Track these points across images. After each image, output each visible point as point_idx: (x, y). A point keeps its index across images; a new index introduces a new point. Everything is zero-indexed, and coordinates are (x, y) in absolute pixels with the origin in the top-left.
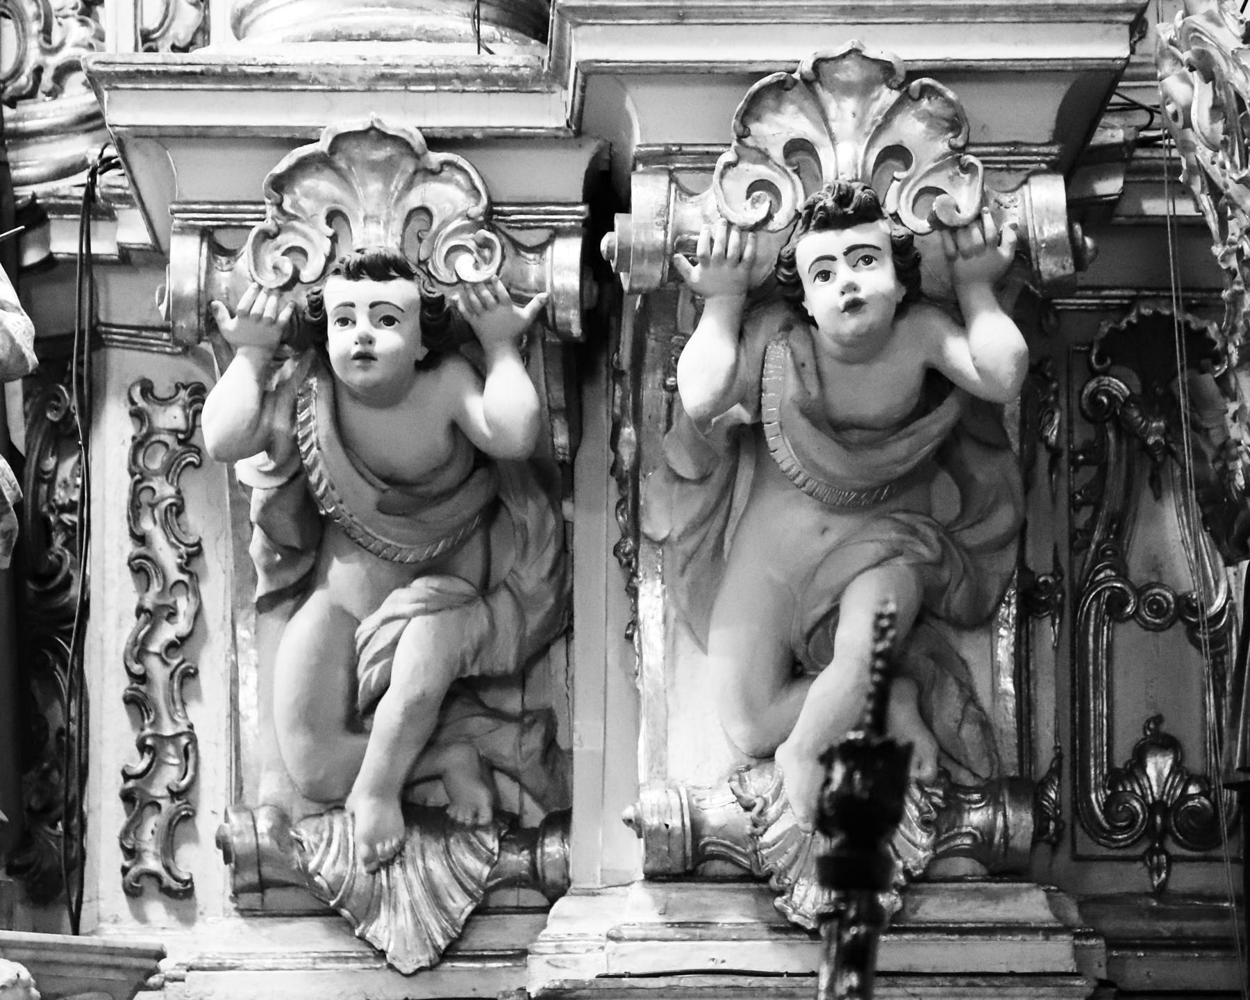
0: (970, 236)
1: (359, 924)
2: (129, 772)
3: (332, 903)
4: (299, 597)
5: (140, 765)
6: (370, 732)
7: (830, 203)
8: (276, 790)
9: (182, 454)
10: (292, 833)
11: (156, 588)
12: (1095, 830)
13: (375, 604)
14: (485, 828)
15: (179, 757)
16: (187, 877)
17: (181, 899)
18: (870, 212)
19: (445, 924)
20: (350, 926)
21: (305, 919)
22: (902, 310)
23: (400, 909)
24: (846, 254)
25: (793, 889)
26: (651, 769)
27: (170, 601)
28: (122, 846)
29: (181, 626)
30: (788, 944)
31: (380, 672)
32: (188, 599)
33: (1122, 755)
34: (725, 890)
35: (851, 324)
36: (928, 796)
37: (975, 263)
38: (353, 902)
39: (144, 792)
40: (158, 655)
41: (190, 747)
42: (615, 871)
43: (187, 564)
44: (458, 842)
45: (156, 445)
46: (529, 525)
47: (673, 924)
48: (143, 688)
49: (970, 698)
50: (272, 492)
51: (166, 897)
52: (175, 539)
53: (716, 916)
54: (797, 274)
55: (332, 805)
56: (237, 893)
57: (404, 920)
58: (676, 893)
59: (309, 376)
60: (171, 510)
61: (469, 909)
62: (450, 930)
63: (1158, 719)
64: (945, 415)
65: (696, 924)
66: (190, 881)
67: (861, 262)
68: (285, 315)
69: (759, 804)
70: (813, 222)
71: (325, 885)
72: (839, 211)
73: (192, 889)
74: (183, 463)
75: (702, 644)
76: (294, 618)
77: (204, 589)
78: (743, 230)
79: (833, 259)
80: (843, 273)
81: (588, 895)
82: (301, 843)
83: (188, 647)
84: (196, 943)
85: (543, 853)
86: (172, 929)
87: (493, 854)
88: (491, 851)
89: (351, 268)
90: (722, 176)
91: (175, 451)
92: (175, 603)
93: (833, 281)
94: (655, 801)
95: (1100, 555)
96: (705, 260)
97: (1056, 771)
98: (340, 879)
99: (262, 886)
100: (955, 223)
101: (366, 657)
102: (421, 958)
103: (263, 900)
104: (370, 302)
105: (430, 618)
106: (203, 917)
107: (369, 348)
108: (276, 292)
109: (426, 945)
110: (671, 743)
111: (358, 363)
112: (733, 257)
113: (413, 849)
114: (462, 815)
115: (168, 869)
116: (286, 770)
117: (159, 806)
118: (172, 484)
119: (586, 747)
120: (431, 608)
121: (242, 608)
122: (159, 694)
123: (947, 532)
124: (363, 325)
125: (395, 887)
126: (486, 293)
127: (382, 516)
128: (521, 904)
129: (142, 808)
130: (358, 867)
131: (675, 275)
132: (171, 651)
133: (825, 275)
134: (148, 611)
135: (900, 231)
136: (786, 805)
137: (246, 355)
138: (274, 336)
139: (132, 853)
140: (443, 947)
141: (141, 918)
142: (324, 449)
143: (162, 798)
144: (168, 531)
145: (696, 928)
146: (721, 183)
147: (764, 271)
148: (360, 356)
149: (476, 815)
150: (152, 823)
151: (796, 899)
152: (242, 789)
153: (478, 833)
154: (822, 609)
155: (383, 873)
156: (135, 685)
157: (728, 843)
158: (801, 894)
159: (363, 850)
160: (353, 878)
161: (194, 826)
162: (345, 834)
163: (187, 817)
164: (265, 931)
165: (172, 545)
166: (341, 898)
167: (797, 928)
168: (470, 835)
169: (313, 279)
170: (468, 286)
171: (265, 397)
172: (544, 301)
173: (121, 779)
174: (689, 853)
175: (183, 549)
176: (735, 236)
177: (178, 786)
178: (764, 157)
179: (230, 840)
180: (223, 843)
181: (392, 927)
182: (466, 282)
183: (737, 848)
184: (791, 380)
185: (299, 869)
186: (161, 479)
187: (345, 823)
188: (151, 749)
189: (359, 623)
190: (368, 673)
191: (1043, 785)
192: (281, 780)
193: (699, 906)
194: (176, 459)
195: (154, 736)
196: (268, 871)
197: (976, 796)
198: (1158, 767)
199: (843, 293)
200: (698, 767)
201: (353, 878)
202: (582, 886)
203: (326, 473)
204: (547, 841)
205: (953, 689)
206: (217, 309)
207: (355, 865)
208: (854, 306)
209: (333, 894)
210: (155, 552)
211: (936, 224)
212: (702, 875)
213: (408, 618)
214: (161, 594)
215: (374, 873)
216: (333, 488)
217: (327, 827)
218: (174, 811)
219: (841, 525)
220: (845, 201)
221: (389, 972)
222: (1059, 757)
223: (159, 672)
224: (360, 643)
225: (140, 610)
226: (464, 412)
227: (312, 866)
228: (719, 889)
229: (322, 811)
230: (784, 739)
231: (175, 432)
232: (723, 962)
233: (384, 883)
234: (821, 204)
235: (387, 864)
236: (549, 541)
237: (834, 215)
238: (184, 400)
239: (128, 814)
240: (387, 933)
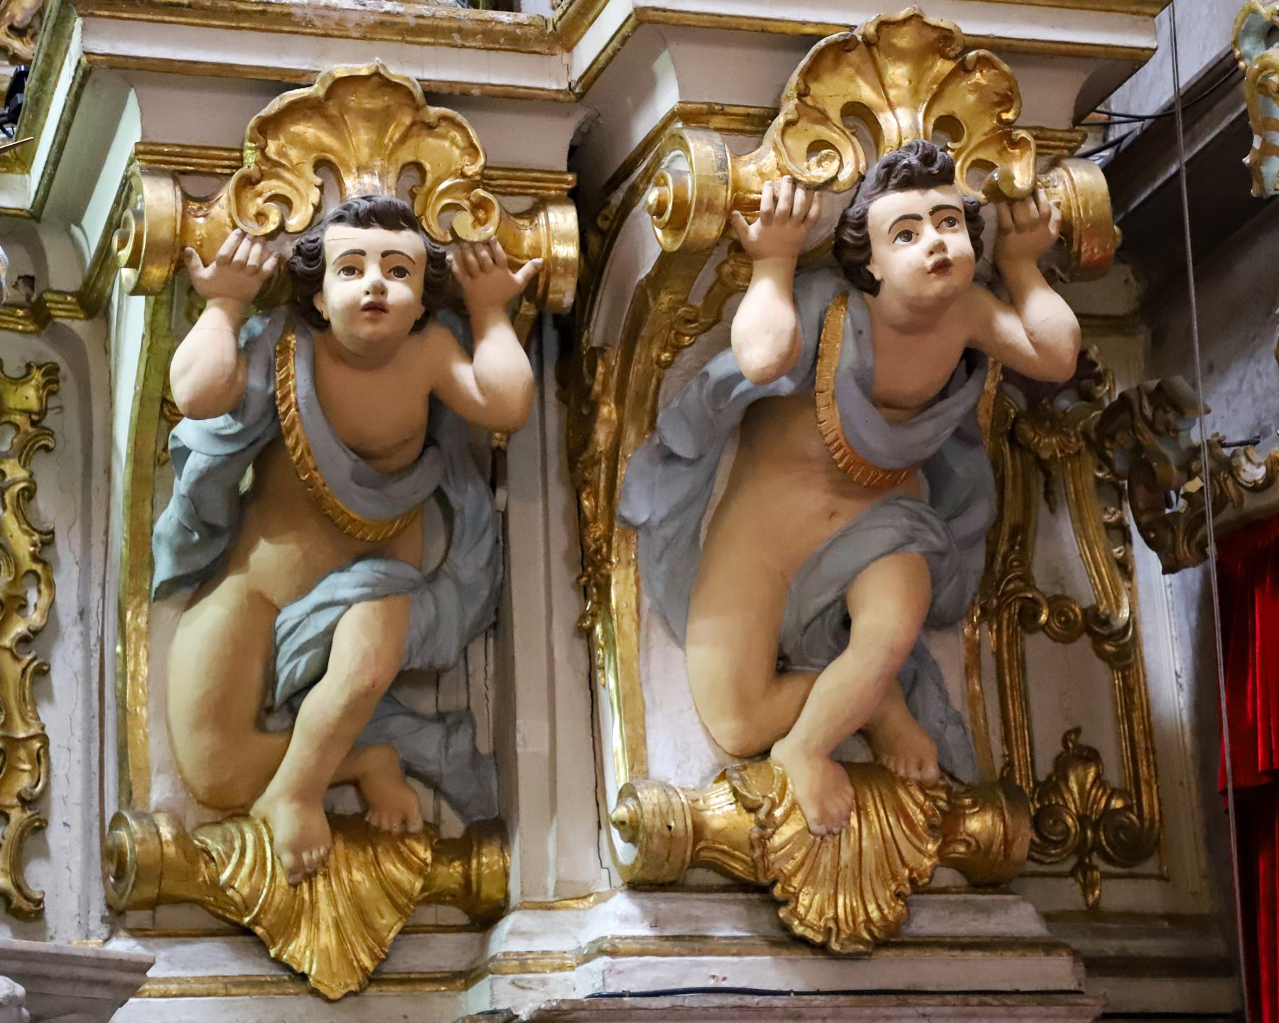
0: (1028, 209)
1: (274, 945)
3: (247, 919)
4: (197, 585)
9: (36, 436)
13: (304, 590)
14: (416, 836)
15: (31, 762)
16: (39, 896)
19: (371, 942)
20: (262, 945)
23: (323, 926)
24: (931, 214)
25: (797, 899)
26: (632, 769)
29: (35, 618)
30: (789, 960)
31: (307, 664)
32: (39, 592)
34: (713, 901)
36: (934, 799)
37: (1028, 238)
40: (10, 650)
42: (571, 882)
44: (388, 851)
45: (7, 426)
46: (467, 511)
47: (667, 938)
50: (219, 460)
52: (29, 526)
53: (709, 929)
54: (867, 236)
55: (230, 813)
57: (327, 938)
58: (665, 904)
59: (286, 332)
60: (23, 494)
61: (397, 927)
62: (377, 950)
65: (692, 938)
66: (41, 901)
67: (944, 224)
68: (269, 265)
70: (893, 181)
74: (37, 446)
75: (678, 638)
76: (196, 608)
77: (58, 580)
78: (811, 188)
79: (918, 218)
80: (929, 235)
81: (541, 908)
82: (209, 853)
83: (38, 642)
85: (480, 864)
87: (426, 864)
88: (424, 861)
89: (361, 215)
91: (26, 432)
93: (916, 242)
94: (655, 801)
96: (768, 218)
100: (1014, 196)
101: (287, 649)
102: (349, 981)
103: (154, 917)
104: (383, 250)
105: (376, 604)
107: (381, 298)
108: (261, 240)
110: (648, 741)
111: (367, 314)
112: (800, 214)
113: (337, 860)
114: (387, 821)
115: (18, 888)
116: (180, 771)
118: (24, 467)
119: (530, 749)
120: (376, 593)
124: (373, 273)
125: (317, 902)
126: (484, 253)
127: (355, 487)
128: (440, 923)
130: (278, 879)
133: (908, 236)
136: (794, 805)
137: (221, 306)
138: (254, 286)
140: (371, 969)
142: (303, 411)
144: (21, 518)
145: (695, 943)
146: (783, 140)
148: (369, 307)
149: (405, 822)
151: (801, 910)
153: (407, 841)
155: (305, 886)
157: (725, 847)
158: (806, 903)
161: (45, 841)
165: (25, 532)
166: (258, 914)
167: (803, 942)
168: (399, 844)
169: (300, 228)
170: (466, 245)
171: (245, 352)
172: (540, 267)
174: (688, 860)
175: (36, 537)
176: (800, 194)
177: (31, 794)
182: (464, 241)
183: (737, 853)
184: (850, 346)
186: (14, 461)
189: (279, 612)
190: (291, 666)
192: (173, 783)
193: (689, 918)
194: (29, 441)
199: (931, 253)
200: (678, 767)
202: (532, 899)
203: (302, 437)
204: (484, 851)
206: (190, 256)
209: (248, 908)
210: (6, 539)
212: (683, 885)
215: (295, 886)
216: (309, 453)
220: (929, 160)
224: (282, 632)
226: (451, 381)
227: (224, 877)
228: (707, 900)
229: (220, 819)
231: (28, 412)
232: (724, 979)
233: (307, 897)
234: (905, 162)
235: (310, 877)
236: (485, 530)
237: (920, 173)
238: (37, 380)
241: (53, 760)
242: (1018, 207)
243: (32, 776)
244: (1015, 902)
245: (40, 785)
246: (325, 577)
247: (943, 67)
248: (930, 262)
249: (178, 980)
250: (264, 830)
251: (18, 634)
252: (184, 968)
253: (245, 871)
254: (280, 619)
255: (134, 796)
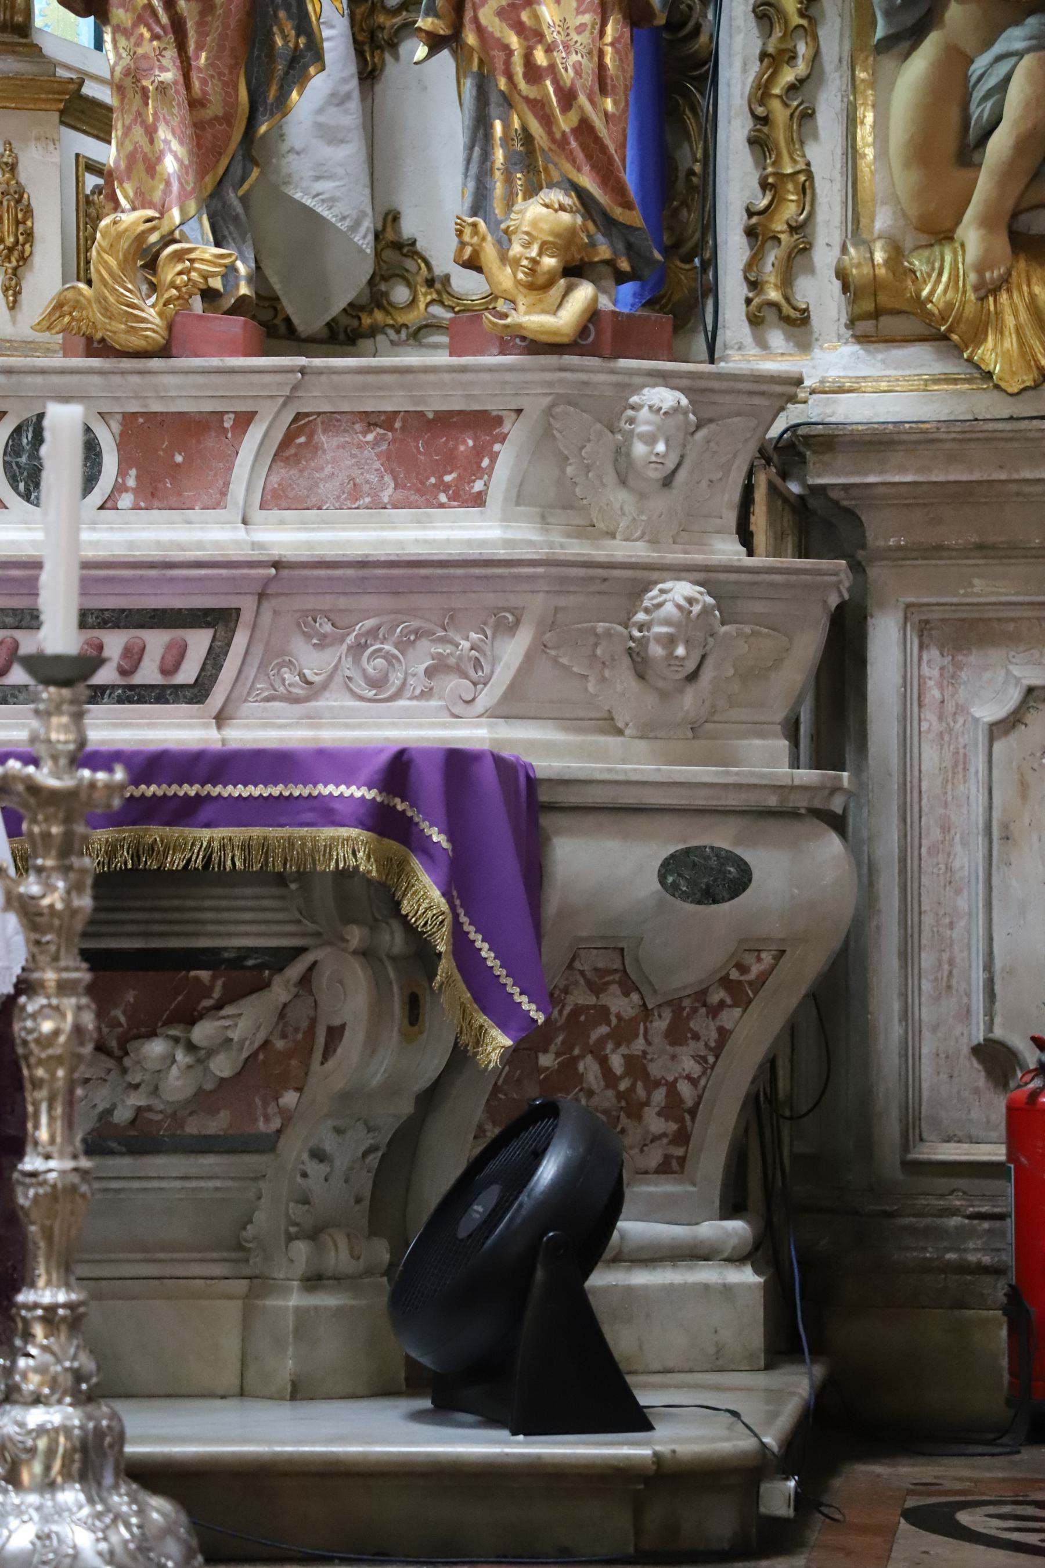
1: (967, 348)
2: (753, 209)
3: (943, 328)
5: (765, 202)
6: (980, 165)
8: (889, 222)
10: (906, 264)
11: (778, 33)
15: (797, 194)
17: (799, 326)
20: (959, 349)
21: (917, 343)
23: (1007, 333)
27: (790, 46)
28: (746, 278)
29: (801, 68)
31: (991, 109)
32: (807, 43)
38: (963, 327)
39: (765, 226)
41: (807, 183)
43: (806, 9)
48: (765, 129)
51: (785, 325)
55: (942, 236)
56: (852, 323)
57: (1010, 343)
71: (936, 312)
73: (808, 317)
77: (821, 33)
82: (914, 272)
83: (807, 87)
84: (814, 367)
86: (790, 355)
92: (795, 47)
98: (950, 305)
99: (877, 314)
101: (978, 94)
102: (1025, 378)
106: (819, 343)
109: (1031, 367)
116: (899, 203)
117: (779, 240)
121: (861, 50)
122: (780, 136)
125: (1002, 312)
129: (764, 243)
132: (791, 92)
134: (770, 55)
139: (754, 285)
141: (762, 344)
143: (782, 232)
150: (772, 256)
152: (858, 222)
155: (991, 299)
156: (758, 127)
159: (973, 277)
160: (963, 304)
161: (811, 259)
162: (955, 261)
163: (805, 249)
164: (880, 357)
166: (952, 323)
173: (746, 216)
177: (796, 221)
179: (849, 272)
180: (841, 274)
181: (999, 350)
185: (912, 296)
187: (955, 253)
188: (772, 186)
189: (972, 62)
192: (894, 213)
195: (775, 174)
196: (883, 299)
201: (963, 304)
207: (964, 292)
209: (944, 320)
213: (1020, 55)
214: (783, 39)
215: (982, 299)
217: (939, 257)
218: (793, 245)
221: (995, 392)
223: (779, 113)
224: (973, 79)
225: (763, 55)
227: (925, 293)
233: (992, 308)
235: (995, 291)
239: (752, 249)
240: (993, 356)
241: (818, 191)
243: (798, 206)
245: (805, 213)
246: (1004, 30)
249: (888, 379)
250: (960, 252)
251: (787, 82)
252: (895, 368)
253: (941, 288)
254: (973, 67)
255: (861, 225)
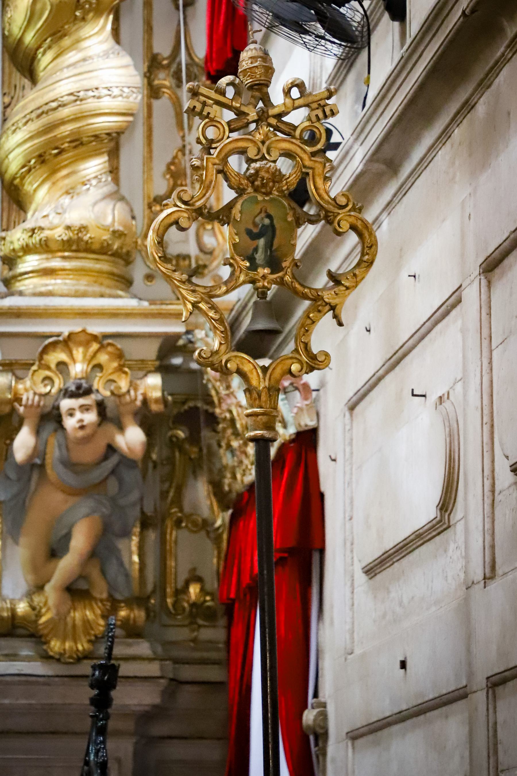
7: (73, 388)
12: (169, 613)
18: (88, 392)
22: (100, 425)
33: (180, 584)
35: (81, 434)
49: (121, 564)
63: (194, 569)
64: (114, 460)
69: (38, 607)
72: (77, 392)
78: (41, 395)
80: (78, 415)
90: (33, 375)
95: (172, 502)
96: (26, 406)
97: (154, 592)
123: (113, 500)
131: (13, 410)
133: (71, 415)
135: (99, 398)
147: (48, 409)
154: (64, 532)
167: (51, 657)
176: (37, 398)
178: (48, 368)
191: (149, 598)
197: (123, 605)
198: (194, 590)
205: (114, 561)
208: (82, 427)
211: (112, 393)
219: (72, 500)
222: (155, 587)
230: (48, 581)
242: (122, 399)
244: (142, 642)
247: (95, 346)
248: (78, 425)
